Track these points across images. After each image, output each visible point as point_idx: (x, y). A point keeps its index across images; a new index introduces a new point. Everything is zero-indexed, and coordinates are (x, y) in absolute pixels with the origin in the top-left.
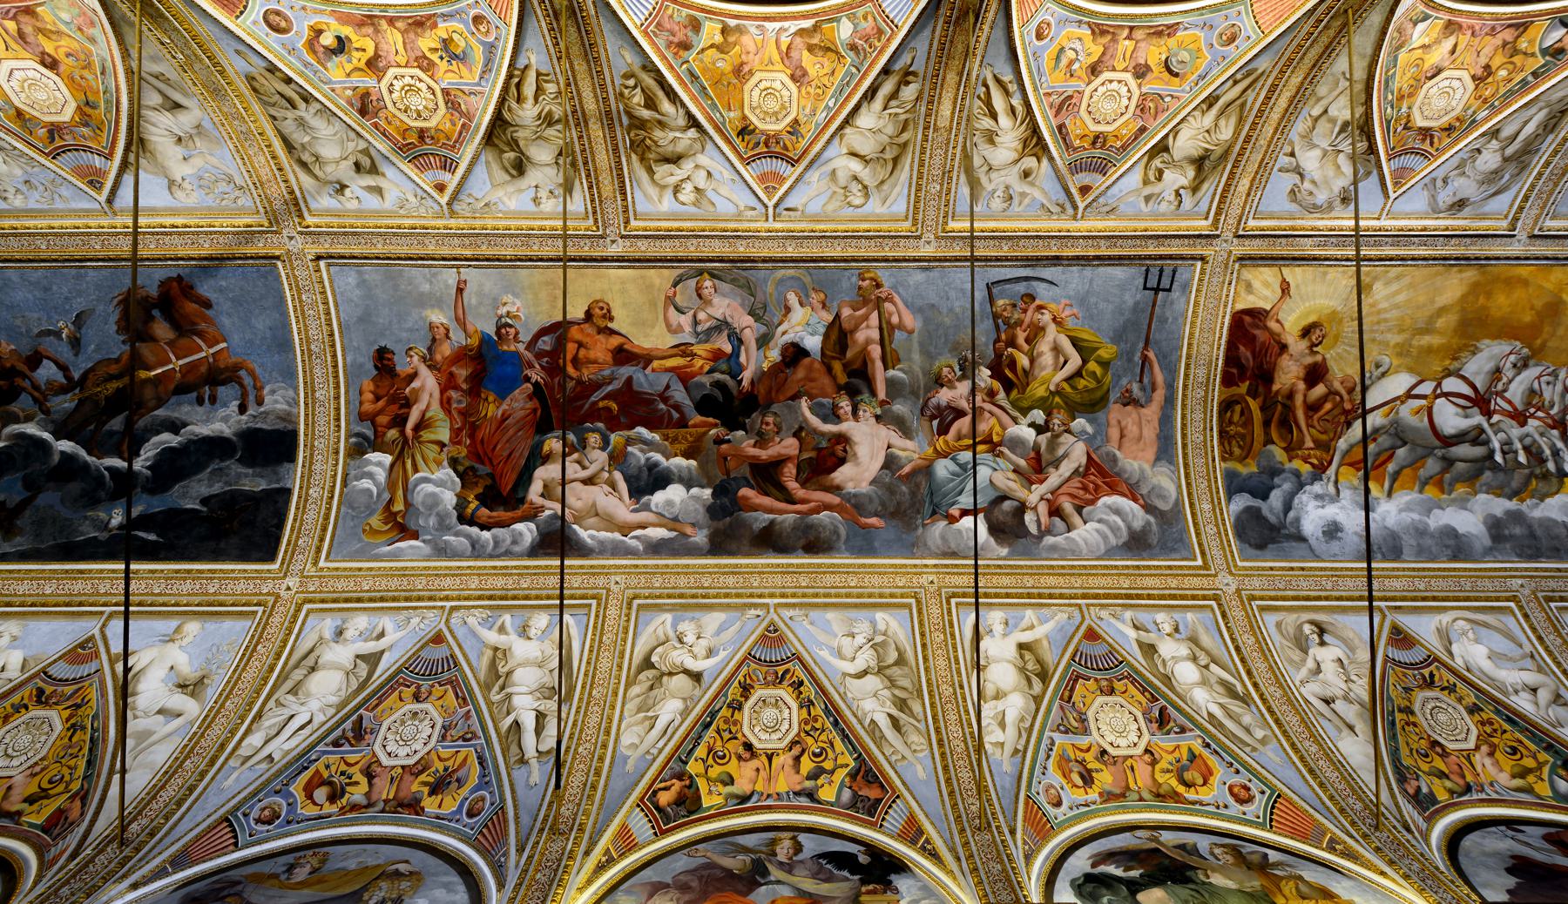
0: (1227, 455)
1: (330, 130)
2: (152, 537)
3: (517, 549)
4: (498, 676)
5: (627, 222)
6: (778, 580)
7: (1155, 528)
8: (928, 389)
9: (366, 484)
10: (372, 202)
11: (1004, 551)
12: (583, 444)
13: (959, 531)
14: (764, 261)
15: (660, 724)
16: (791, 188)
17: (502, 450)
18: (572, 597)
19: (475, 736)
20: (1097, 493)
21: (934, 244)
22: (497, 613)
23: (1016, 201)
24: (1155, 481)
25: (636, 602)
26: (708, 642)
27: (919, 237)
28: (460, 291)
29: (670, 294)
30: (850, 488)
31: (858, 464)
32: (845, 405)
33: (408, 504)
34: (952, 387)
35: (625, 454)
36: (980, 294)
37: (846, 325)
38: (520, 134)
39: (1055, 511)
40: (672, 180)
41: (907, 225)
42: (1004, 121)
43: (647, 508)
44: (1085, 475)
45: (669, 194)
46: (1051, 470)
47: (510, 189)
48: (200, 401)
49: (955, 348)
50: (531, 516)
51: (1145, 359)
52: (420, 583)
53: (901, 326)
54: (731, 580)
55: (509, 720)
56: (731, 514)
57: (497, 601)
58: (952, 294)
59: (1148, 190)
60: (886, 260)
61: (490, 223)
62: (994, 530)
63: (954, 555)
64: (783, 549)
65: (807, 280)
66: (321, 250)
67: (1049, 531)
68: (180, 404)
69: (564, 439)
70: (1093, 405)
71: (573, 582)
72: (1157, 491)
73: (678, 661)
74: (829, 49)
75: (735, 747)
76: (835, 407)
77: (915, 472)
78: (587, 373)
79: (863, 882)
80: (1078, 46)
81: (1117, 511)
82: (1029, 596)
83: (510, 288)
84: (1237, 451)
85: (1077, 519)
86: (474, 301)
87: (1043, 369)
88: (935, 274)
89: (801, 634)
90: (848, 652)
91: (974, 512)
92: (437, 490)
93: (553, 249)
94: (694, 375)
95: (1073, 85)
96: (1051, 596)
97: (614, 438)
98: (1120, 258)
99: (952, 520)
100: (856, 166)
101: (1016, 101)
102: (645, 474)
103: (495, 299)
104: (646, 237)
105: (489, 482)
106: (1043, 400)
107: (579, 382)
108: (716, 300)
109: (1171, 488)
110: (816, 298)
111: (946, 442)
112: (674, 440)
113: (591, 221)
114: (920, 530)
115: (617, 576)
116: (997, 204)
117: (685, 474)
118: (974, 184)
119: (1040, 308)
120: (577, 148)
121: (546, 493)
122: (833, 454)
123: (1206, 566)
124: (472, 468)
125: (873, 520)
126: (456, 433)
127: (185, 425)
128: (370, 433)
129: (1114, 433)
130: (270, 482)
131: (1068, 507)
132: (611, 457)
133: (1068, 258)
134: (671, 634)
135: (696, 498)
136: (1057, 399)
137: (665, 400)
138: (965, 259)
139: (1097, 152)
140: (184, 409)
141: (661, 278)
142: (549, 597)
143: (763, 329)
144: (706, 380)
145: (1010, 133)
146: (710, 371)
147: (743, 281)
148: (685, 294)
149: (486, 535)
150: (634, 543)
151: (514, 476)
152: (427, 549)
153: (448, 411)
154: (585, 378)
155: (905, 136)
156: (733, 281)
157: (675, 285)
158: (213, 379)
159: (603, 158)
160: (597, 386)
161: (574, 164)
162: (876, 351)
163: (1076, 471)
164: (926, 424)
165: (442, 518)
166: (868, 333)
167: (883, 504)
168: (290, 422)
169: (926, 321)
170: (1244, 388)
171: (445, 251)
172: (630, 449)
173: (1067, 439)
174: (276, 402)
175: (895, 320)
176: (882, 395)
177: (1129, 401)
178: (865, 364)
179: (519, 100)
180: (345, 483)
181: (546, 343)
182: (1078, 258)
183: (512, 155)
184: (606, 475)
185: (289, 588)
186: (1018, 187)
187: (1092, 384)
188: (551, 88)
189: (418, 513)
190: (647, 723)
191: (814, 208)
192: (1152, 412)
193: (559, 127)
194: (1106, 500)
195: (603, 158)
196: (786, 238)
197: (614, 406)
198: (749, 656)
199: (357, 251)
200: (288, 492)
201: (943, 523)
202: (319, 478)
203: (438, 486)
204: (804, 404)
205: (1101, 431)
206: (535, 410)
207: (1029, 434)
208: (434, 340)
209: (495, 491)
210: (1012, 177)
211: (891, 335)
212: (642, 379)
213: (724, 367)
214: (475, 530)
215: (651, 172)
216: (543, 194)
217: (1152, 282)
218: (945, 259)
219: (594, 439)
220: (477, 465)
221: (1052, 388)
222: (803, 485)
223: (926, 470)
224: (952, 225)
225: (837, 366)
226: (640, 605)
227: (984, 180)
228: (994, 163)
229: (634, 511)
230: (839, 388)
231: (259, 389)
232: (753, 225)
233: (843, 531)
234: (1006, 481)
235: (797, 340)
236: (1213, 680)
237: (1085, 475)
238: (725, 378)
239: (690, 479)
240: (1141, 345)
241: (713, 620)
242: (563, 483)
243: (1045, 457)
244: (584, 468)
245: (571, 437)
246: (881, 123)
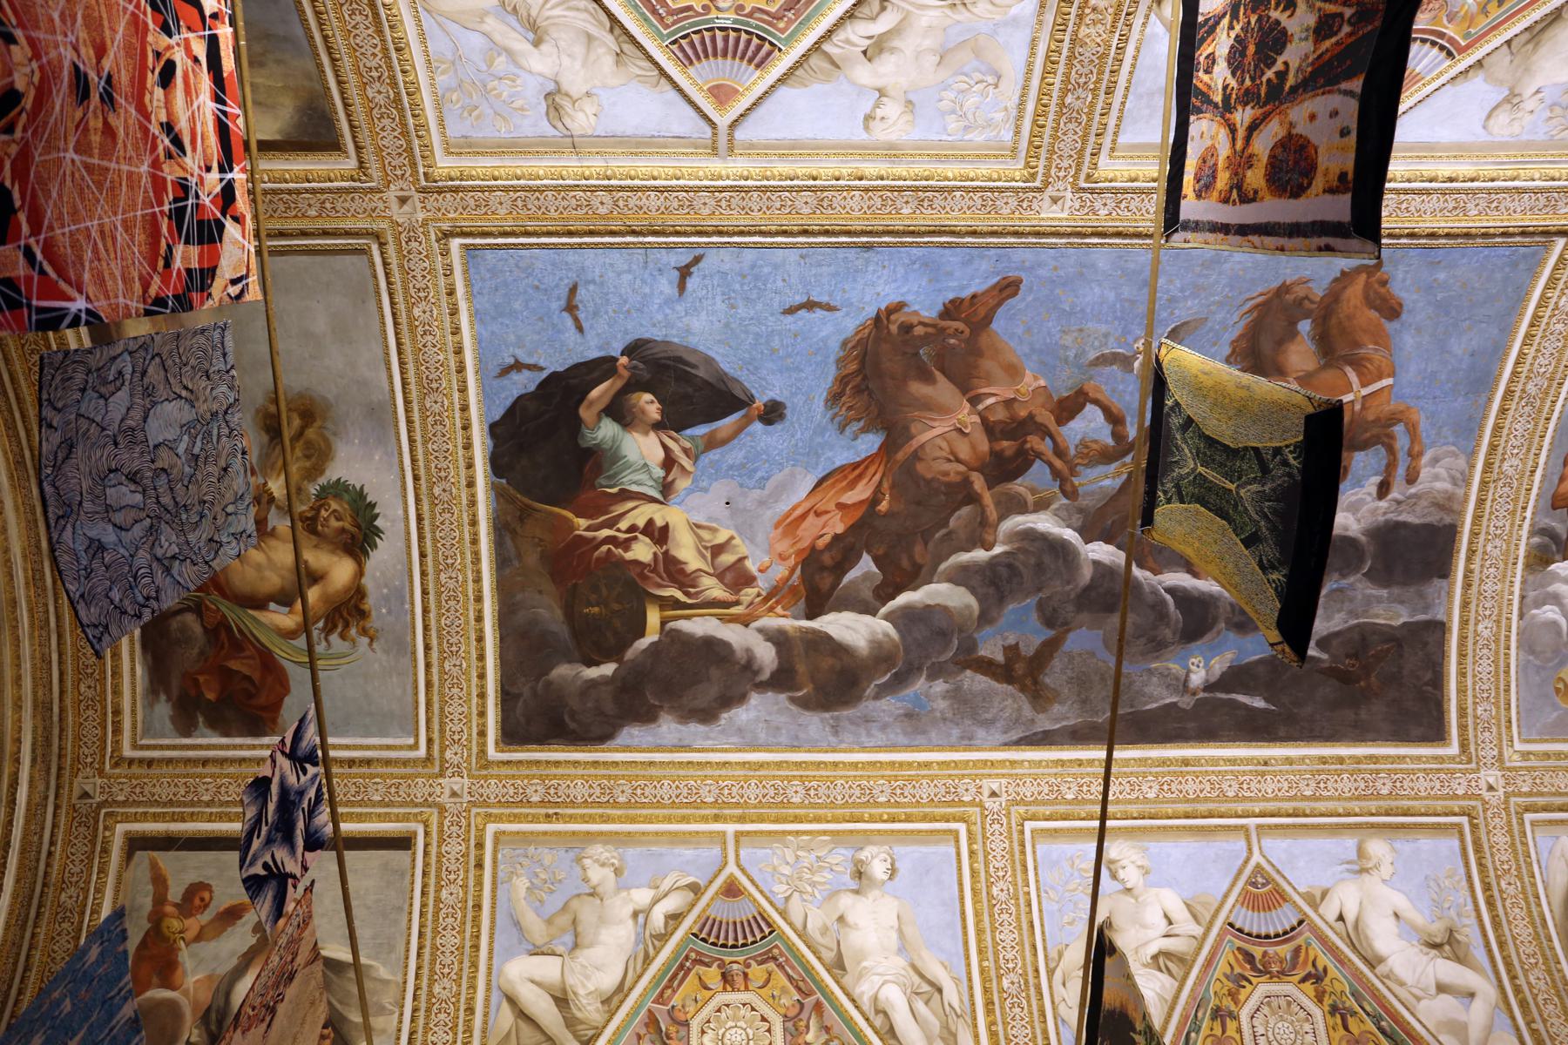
2: (1259, 703)
130: (1414, 612)
168: (1450, 511)
174: (1436, 478)
185: (1491, 788)
200: (1440, 628)
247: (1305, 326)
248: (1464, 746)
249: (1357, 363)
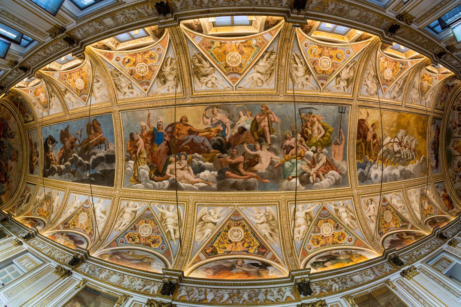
0: (358, 158)
1: (124, 80)
3: (164, 188)
4: (163, 219)
5: (192, 93)
6: (238, 198)
7: (341, 179)
8: (283, 141)
9: (129, 169)
10: (131, 96)
11: (304, 188)
12: (180, 159)
13: (292, 183)
14: (232, 102)
15: (206, 235)
16: (240, 81)
17: (159, 160)
18: (180, 201)
19: (160, 233)
20: (328, 170)
21: (283, 97)
22: (161, 204)
23: (305, 86)
24: (342, 166)
25: (197, 204)
26: (218, 215)
27: (279, 95)
28: (149, 116)
29: (204, 113)
30: (260, 171)
31: (262, 164)
32: (258, 146)
33: (138, 174)
34: (290, 140)
35: (192, 161)
36: (297, 112)
37: (258, 121)
38: (166, 73)
39: (318, 176)
40: (205, 81)
41: (275, 91)
42: (300, 65)
43: (198, 177)
44: (326, 165)
45: (204, 85)
46: (317, 164)
47: (162, 88)
48: (99, 148)
49: (291, 128)
50: (167, 179)
51: (340, 131)
52: (143, 195)
53: (274, 121)
54: (224, 198)
55: (167, 230)
56: (224, 179)
57: (162, 201)
58: (289, 112)
59: (337, 86)
60: (269, 102)
61: (157, 97)
62: (302, 182)
63: (290, 190)
64: (239, 189)
65: (246, 107)
66: (120, 109)
67: (316, 182)
69: (175, 157)
70: (327, 145)
71: (180, 197)
72: (342, 169)
73: (209, 220)
74: (250, 46)
75: (226, 241)
76: (255, 146)
77: (279, 166)
78: (181, 138)
79: (260, 269)
80: (315, 49)
81: (333, 175)
82: (309, 200)
83: (161, 115)
84: (360, 157)
85: (323, 178)
86: (152, 119)
87: (315, 134)
88: (283, 106)
89: (245, 213)
90: (258, 217)
91: (296, 177)
92: (145, 171)
93: (173, 102)
94: (211, 137)
95: (316, 58)
96: (315, 199)
97: (189, 156)
98: (333, 103)
99: (290, 180)
100: (259, 75)
101: (302, 60)
102: (198, 167)
103: (157, 118)
104: (197, 97)
105: (156, 169)
106: (315, 143)
107: (179, 140)
108: (218, 114)
109: (345, 167)
110: (248, 113)
111: (288, 157)
112: (206, 157)
113: (182, 94)
114: (280, 183)
115: (191, 196)
116: (300, 87)
117: (209, 167)
118: (293, 81)
119: (314, 116)
120: (180, 75)
121: (171, 172)
122: (254, 161)
123: (351, 188)
124: (152, 165)
125: (267, 181)
126: (148, 155)
128: (129, 155)
129: (333, 153)
131: (321, 174)
132: (188, 162)
133: (320, 103)
134: (207, 212)
135: (213, 174)
136: (319, 143)
137: (203, 145)
138: (292, 102)
139: (324, 75)
141: (201, 109)
142: (173, 201)
143: (232, 123)
144: (215, 139)
145: (302, 69)
146: (216, 136)
147: (226, 109)
148: (209, 113)
149: (157, 183)
150: (195, 187)
151: (162, 168)
152: (143, 186)
153: (146, 149)
154: (180, 139)
155: (273, 68)
156: (223, 109)
157: (206, 110)
158: (101, 142)
159: (186, 77)
160: (183, 141)
161: (179, 79)
162: (267, 129)
163: (323, 164)
164: (282, 151)
165: (146, 178)
166: (264, 123)
167: (269, 175)
169: (282, 120)
170: (361, 140)
171: (146, 106)
172: (193, 160)
173: (321, 155)
175: (273, 119)
176: (269, 142)
177: (336, 144)
178: (264, 133)
179: (166, 66)
180: (125, 169)
181: (170, 129)
182: (322, 103)
183: (163, 79)
184: (187, 167)
186: (305, 82)
187: (328, 139)
188: (174, 61)
189: (141, 177)
190: (202, 234)
191: (247, 87)
192: (342, 147)
193: (176, 70)
194: (330, 172)
195: (186, 77)
196: (239, 95)
197: (188, 147)
198: (230, 219)
199: (127, 108)
200: (114, 170)
201: (287, 181)
203: (145, 170)
204: (245, 145)
205: (330, 151)
206: (167, 149)
207: (311, 153)
208: (143, 130)
209: (158, 172)
210: (303, 79)
211: (272, 124)
212: (196, 139)
213: (221, 134)
214: (154, 182)
215: (199, 79)
216: (170, 88)
217: (341, 111)
218: (287, 102)
219: (183, 157)
220: (153, 164)
221: (318, 140)
222: (245, 170)
223: (282, 165)
224: (288, 92)
225: (255, 134)
226: (197, 205)
227: (296, 80)
228: (298, 76)
229: (195, 178)
230: (256, 140)
231: (108, 145)
232: (229, 92)
233: (257, 184)
234: (305, 168)
235: (243, 126)
236: (349, 216)
237: (326, 165)
238: (221, 138)
239: (211, 169)
240: (339, 128)
241: (219, 209)
242: (176, 169)
243: (316, 160)
244: (181, 165)
245: (177, 156)
246: (266, 64)
249: (98, 132)
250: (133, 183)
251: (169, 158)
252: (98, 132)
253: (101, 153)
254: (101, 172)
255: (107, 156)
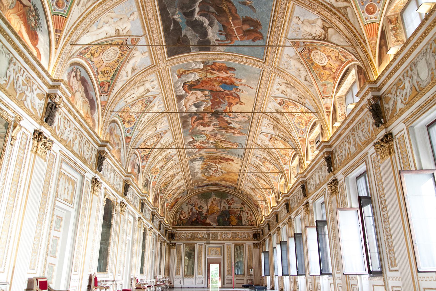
2: (171, 28)
9: (193, 65)
33: (188, 74)
48: (220, 31)
68: (219, 26)
92: (193, 77)
127: (212, 27)
140: (217, 26)
152: (175, 81)
158: (227, 34)
165: (185, 80)
200: (190, 51)
202: (194, 59)
203: (193, 77)
214: (182, 86)
247: (252, 28)
248: (168, 60)
249: (244, 35)
250: (177, 73)
251: (206, 90)
252: (244, 35)
253: (213, 34)
254: (185, 36)
255: (208, 42)
